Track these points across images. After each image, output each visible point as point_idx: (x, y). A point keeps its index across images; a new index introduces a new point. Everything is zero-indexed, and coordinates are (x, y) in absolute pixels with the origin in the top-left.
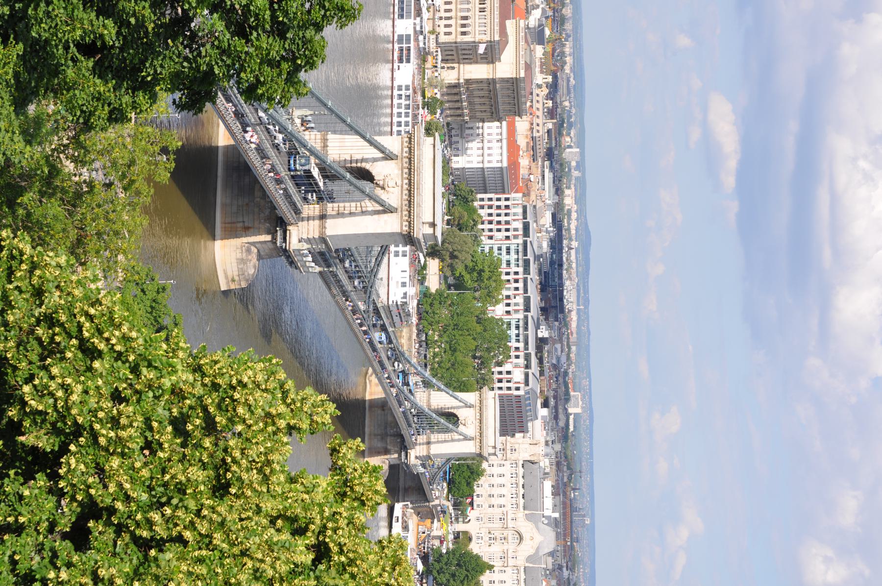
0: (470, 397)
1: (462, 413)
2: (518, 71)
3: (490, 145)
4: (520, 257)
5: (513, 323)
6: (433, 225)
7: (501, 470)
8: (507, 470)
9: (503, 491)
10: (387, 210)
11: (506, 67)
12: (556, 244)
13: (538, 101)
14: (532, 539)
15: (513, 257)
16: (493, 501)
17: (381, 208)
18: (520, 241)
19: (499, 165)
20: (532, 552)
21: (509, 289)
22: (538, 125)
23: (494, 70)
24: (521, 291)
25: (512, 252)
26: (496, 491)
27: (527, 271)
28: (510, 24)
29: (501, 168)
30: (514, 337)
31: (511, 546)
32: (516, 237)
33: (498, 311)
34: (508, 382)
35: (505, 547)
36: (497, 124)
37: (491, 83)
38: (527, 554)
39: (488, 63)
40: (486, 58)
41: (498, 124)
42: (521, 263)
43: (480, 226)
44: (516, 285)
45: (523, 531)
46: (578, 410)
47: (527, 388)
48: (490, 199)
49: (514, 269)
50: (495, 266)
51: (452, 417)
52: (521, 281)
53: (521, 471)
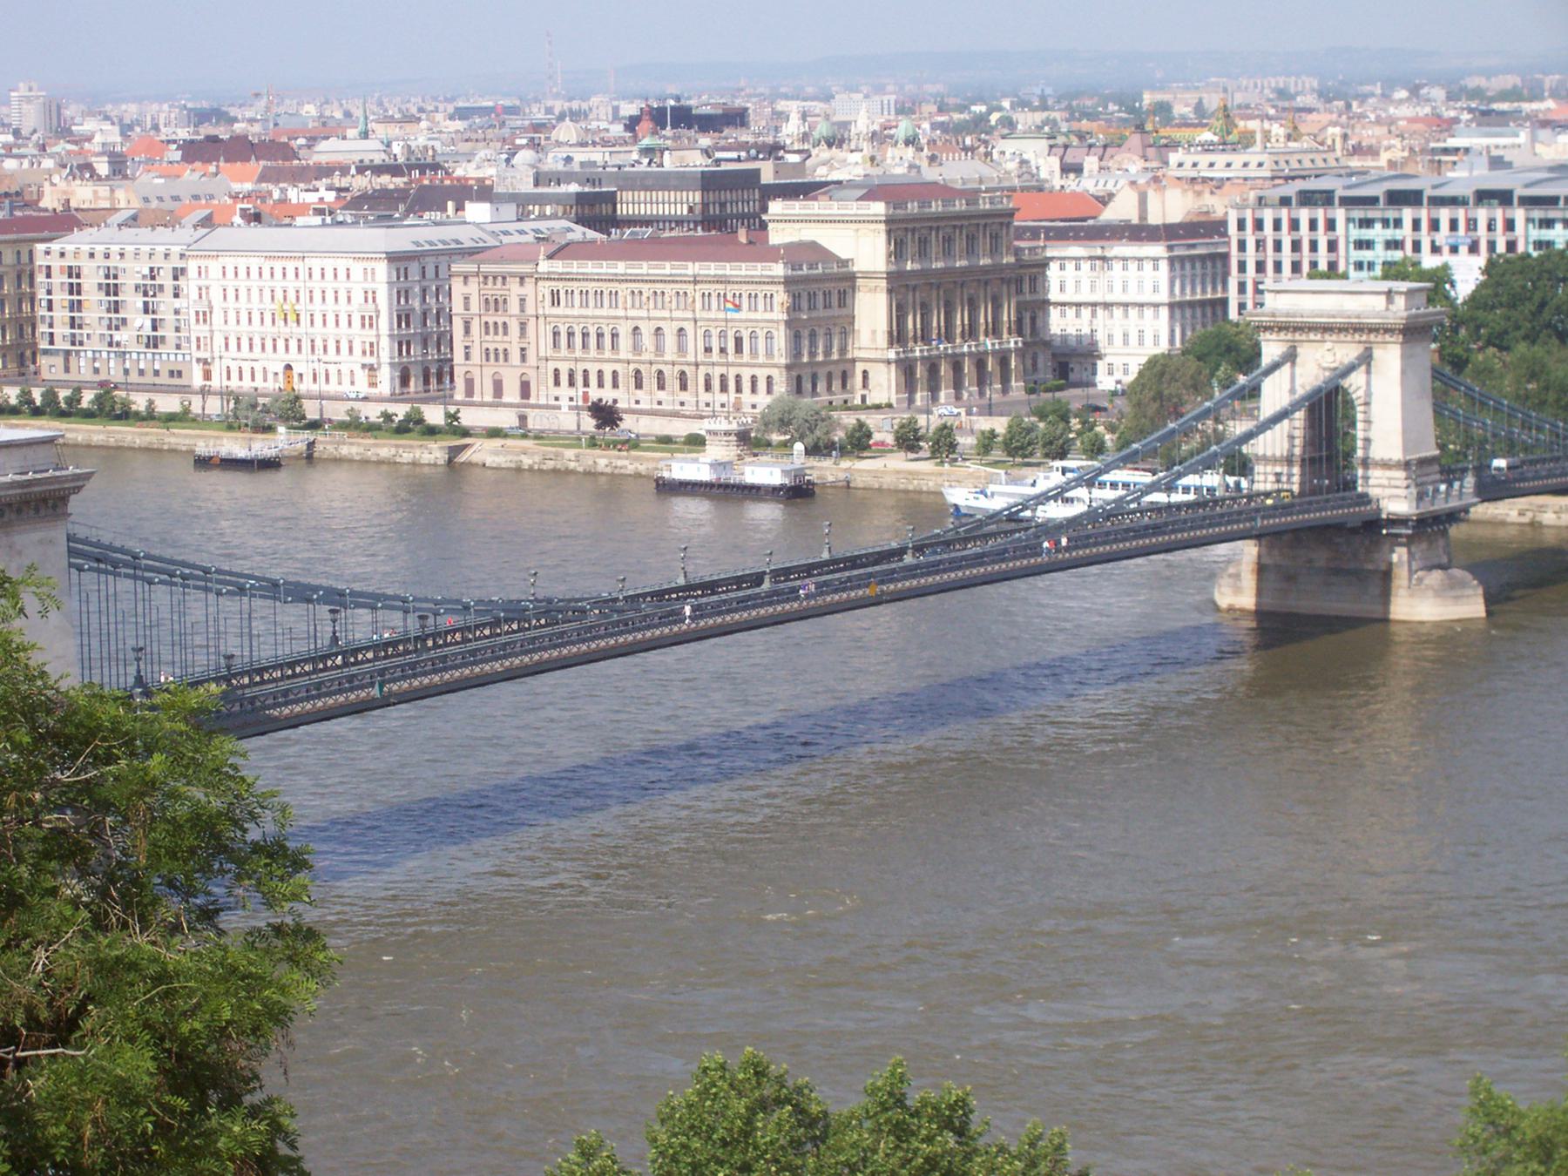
3: (1118, 287)
15: (1378, 233)
18: (1340, 214)
19: (1164, 265)
23: (868, 275)
24: (1461, 214)
25: (1366, 234)
29: (1171, 260)
32: (1331, 225)
36: (1053, 272)
37: (898, 283)
39: (853, 288)
41: (1054, 267)
42: (1391, 214)
44: (1444, 225)
48: (1242, 288)
49: (1406, 232)
52: (1435, 213)
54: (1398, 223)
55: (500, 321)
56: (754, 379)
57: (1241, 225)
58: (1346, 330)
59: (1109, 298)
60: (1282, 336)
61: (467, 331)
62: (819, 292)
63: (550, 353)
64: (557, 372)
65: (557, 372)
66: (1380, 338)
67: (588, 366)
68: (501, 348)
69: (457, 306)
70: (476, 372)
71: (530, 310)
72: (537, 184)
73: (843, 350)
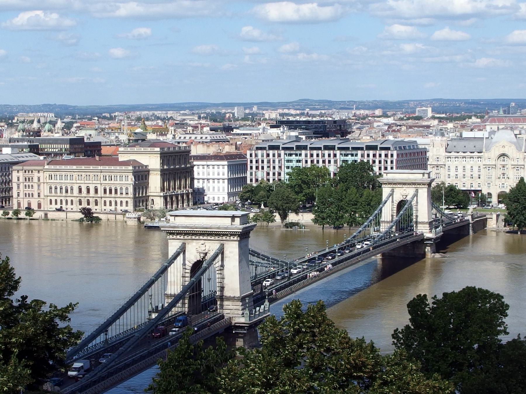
0: (386, 191)
1: (398, 197)
2: (155, 153)
4: (294, 152)
5: (343, 158)
6: (233, 218)
7: (453, 169)
8: (452, 163)
9: (468, 167)
10: (221, 252)
11: (152, 161)
12: (292, 125)
13: (185, 138)
14: (504, 147)
16: (476, 175)
17: (220, 256)
18: (282, 152)
19: (226, 167)
20: (513, 147)
21: (318, 162)
22: (201, 138)
23: (154, 170)
24: (320, 152)
26: (468, 173)
27: (305, 148)
28: (121, 159)
29: (228, 166)
30: (354, 158)
31: (509, 162)
33: (332, 169)
34: (387, 163)
35: (509, 166)
36: (195, 169)
38: (515, 151)
40: (146, 176)
42: (298, 152)
43: (271, 181)
44: (315, 156)
45: (498, 153)
46: (430, 110)
47: (392, 148)
48: (251, 174)
50: (299, 171)
51: (401, 204)
53: (453, 154)
54: (300, 155)
55: (30, 184)
56: (121, 202)
57: (251, 155)
58: (410, 184)
59: (209, 177)
60: (389, 186)
61: (18, 187)
62: (141, 175)
63: (48, 194)
64: (51, 200)
65: (51, 200)
66: (421, 186)
67: (62, 198)
68: (31, 193)
69: (15, 179)
70: (21, 201)
71: (41, 181)
72: (10, 142)
73: (146, 193)
